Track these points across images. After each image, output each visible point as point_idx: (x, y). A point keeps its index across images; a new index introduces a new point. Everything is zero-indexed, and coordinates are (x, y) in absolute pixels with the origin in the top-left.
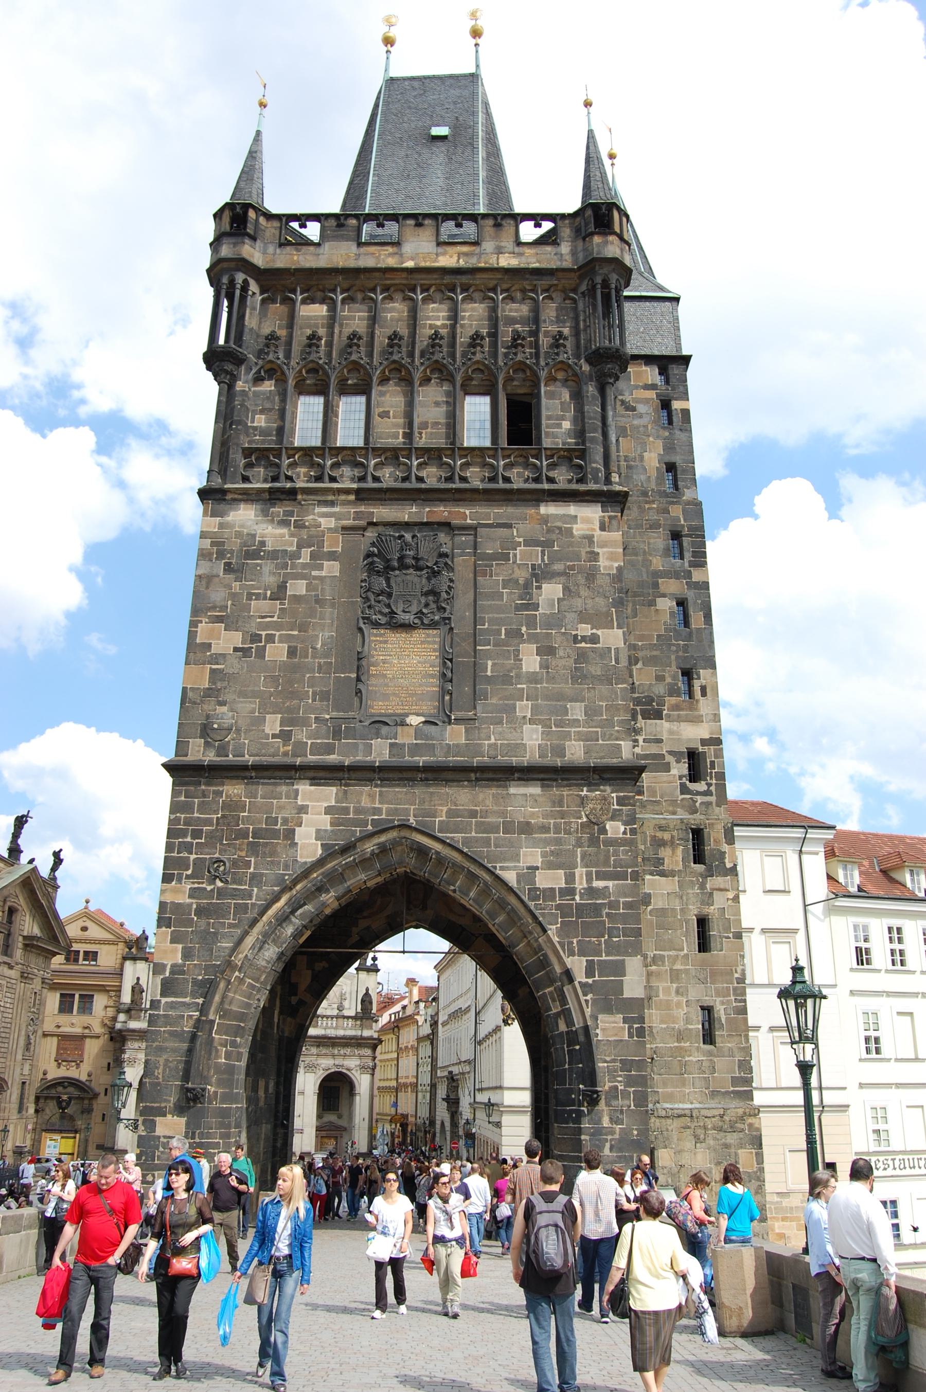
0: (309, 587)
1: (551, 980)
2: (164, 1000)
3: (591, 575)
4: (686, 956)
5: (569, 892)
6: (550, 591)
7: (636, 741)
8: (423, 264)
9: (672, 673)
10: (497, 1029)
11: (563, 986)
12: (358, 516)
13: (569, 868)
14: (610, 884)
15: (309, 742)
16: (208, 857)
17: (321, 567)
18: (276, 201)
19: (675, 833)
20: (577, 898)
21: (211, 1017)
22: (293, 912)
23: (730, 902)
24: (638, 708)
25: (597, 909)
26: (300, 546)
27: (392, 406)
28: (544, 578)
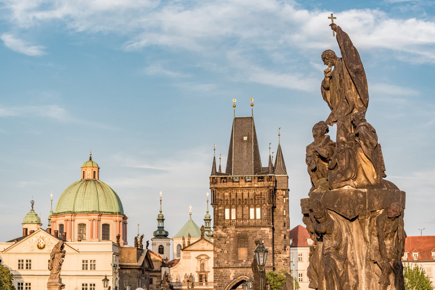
3: (268, 239)
9: (283, 247)
12: (235, 231)
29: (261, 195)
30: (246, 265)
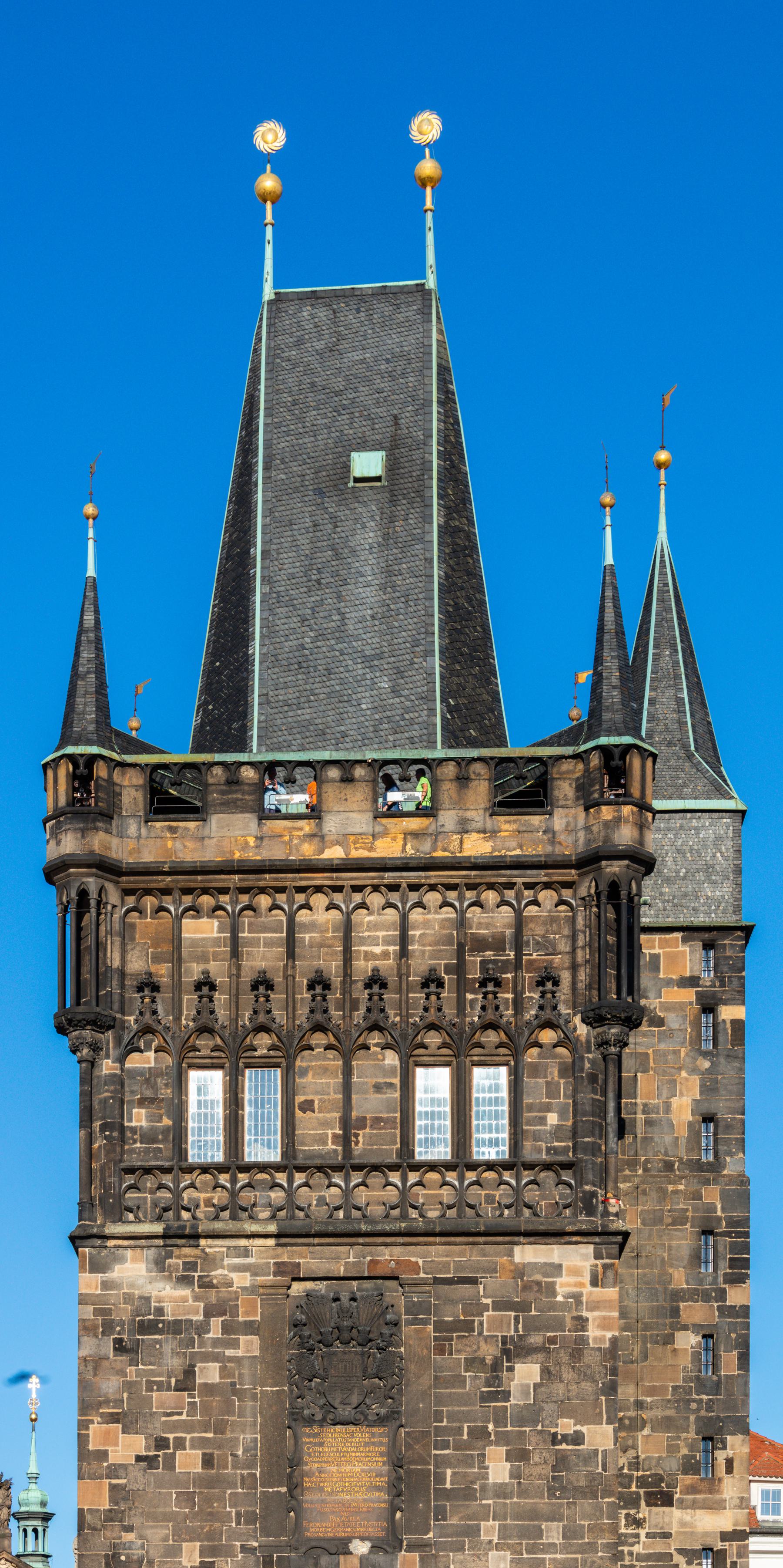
6: (526, 1373)
7: (637, 1536)
24: (642, 1491)
27: (317, 1093)
28: (518, 1356)
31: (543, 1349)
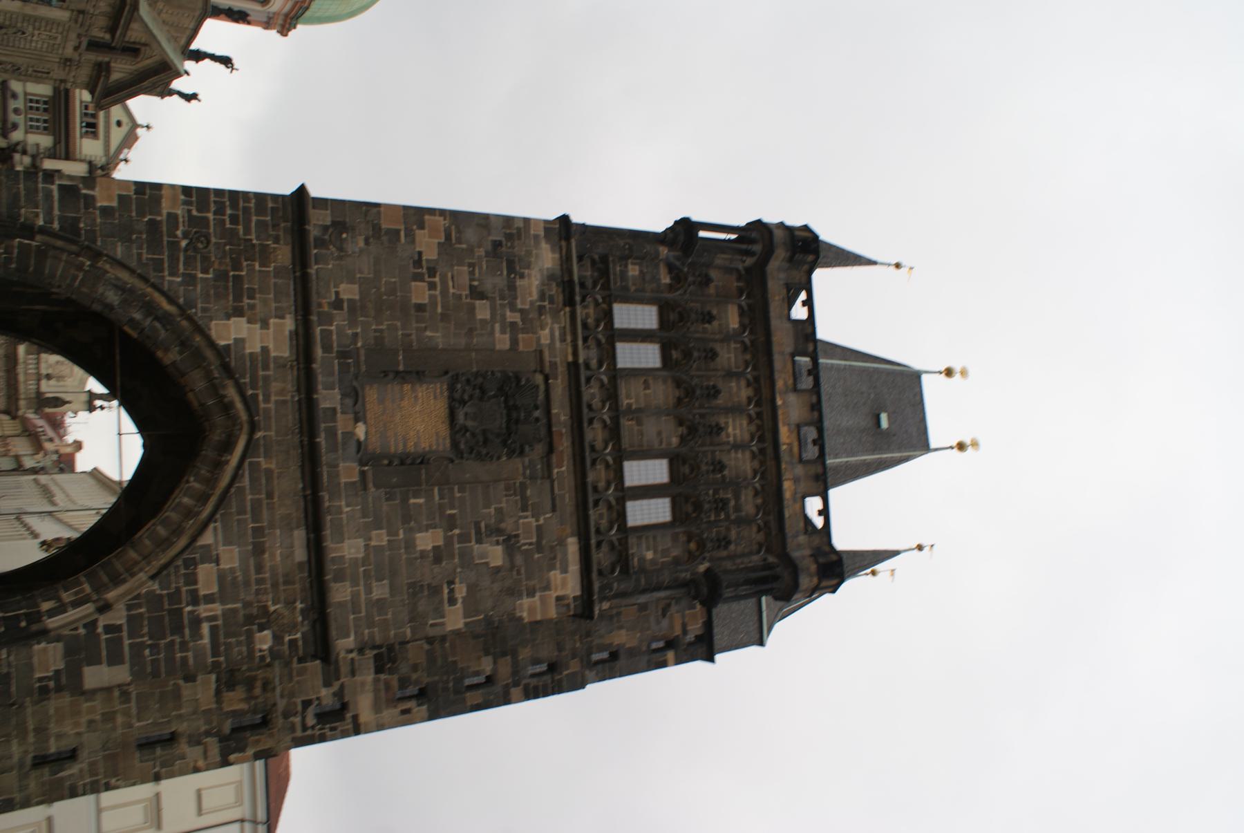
0: (483, 321)
1: (99, 588)
2: (55, 188)
3: (513, 592)
4: (131, 726)
5: (195, 599)
6: (495, 555)
7: (351, 651)
8: (780, 412)
10: (35, 535)
11: (94, 602)
12: (553, 365)
13: (222, 597)
14: (206, 640)
15: (333, 328)
16: (211, 230)
17: (503, 332)
18: (822, 278)
19: (261, 700)
20: (189, 608)
21: (38, 237)
22: (157, 318)
23: (192, 765)
25: (178, 629)
26: (522, 311)
29: (740, 522)
30: (333, 448)
31: (513, 566)
